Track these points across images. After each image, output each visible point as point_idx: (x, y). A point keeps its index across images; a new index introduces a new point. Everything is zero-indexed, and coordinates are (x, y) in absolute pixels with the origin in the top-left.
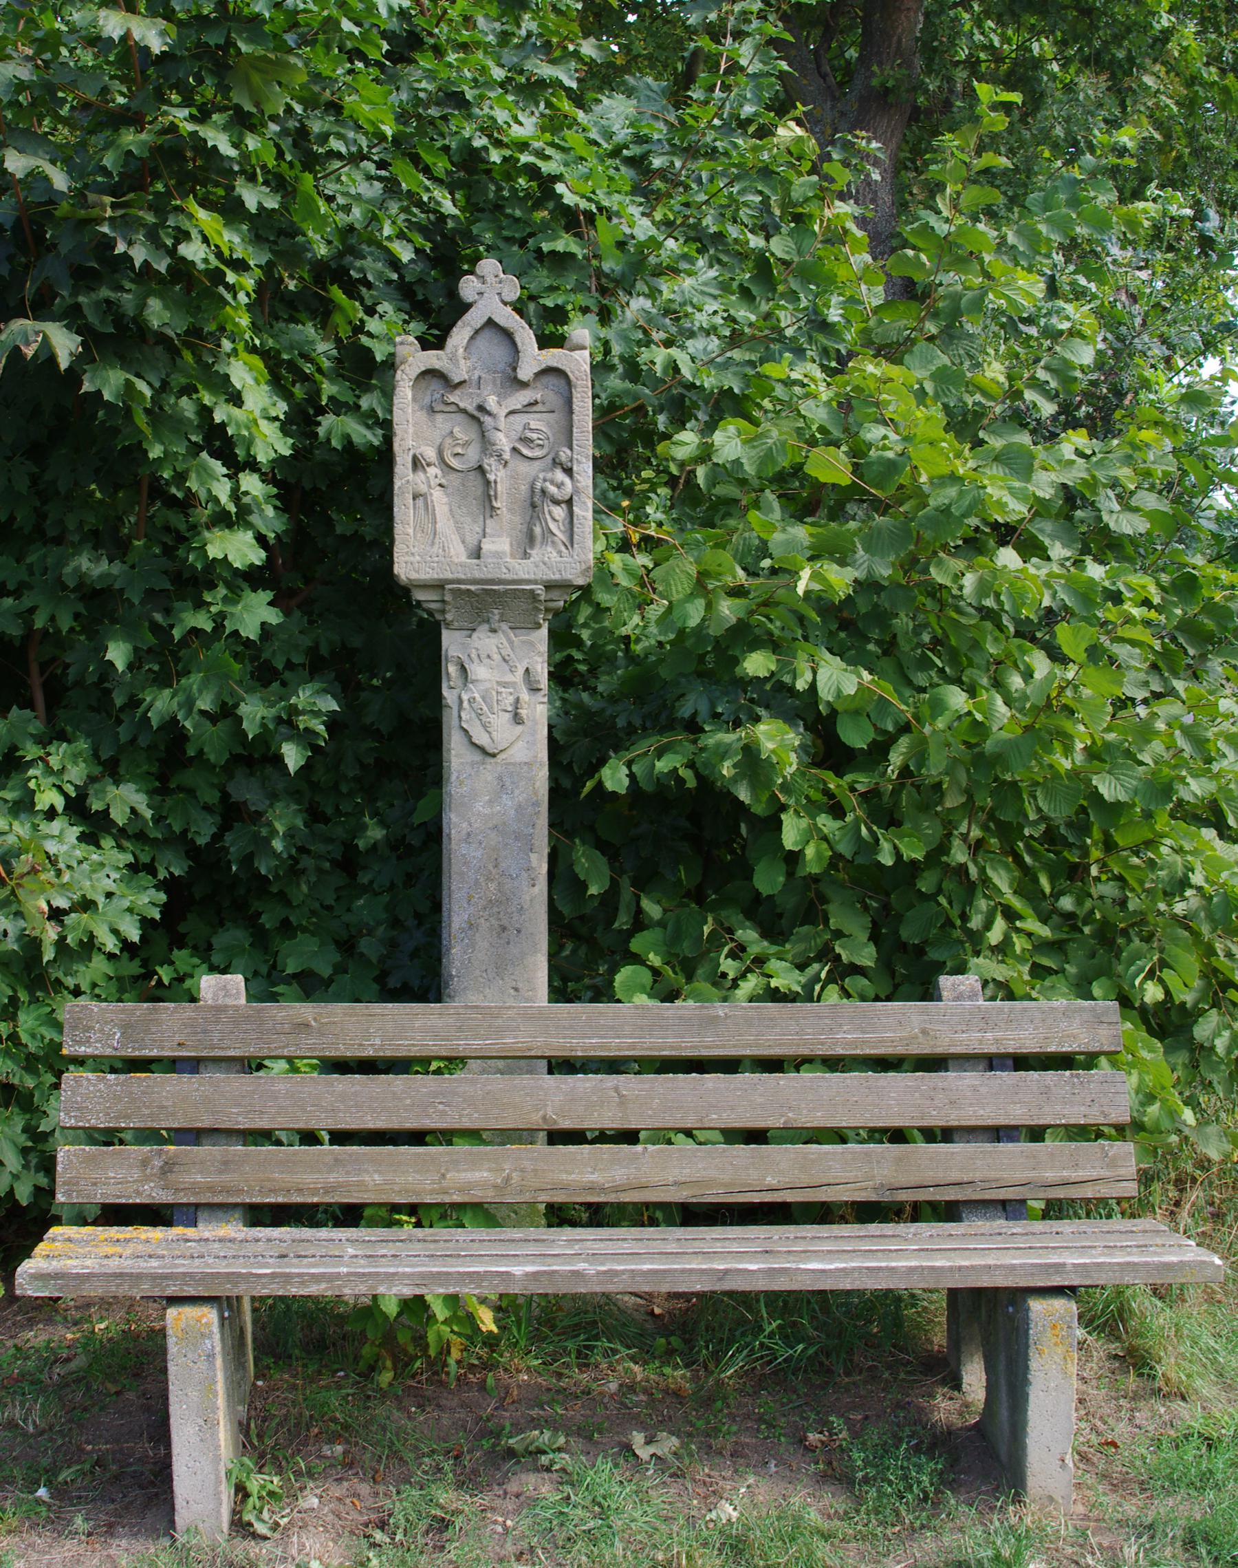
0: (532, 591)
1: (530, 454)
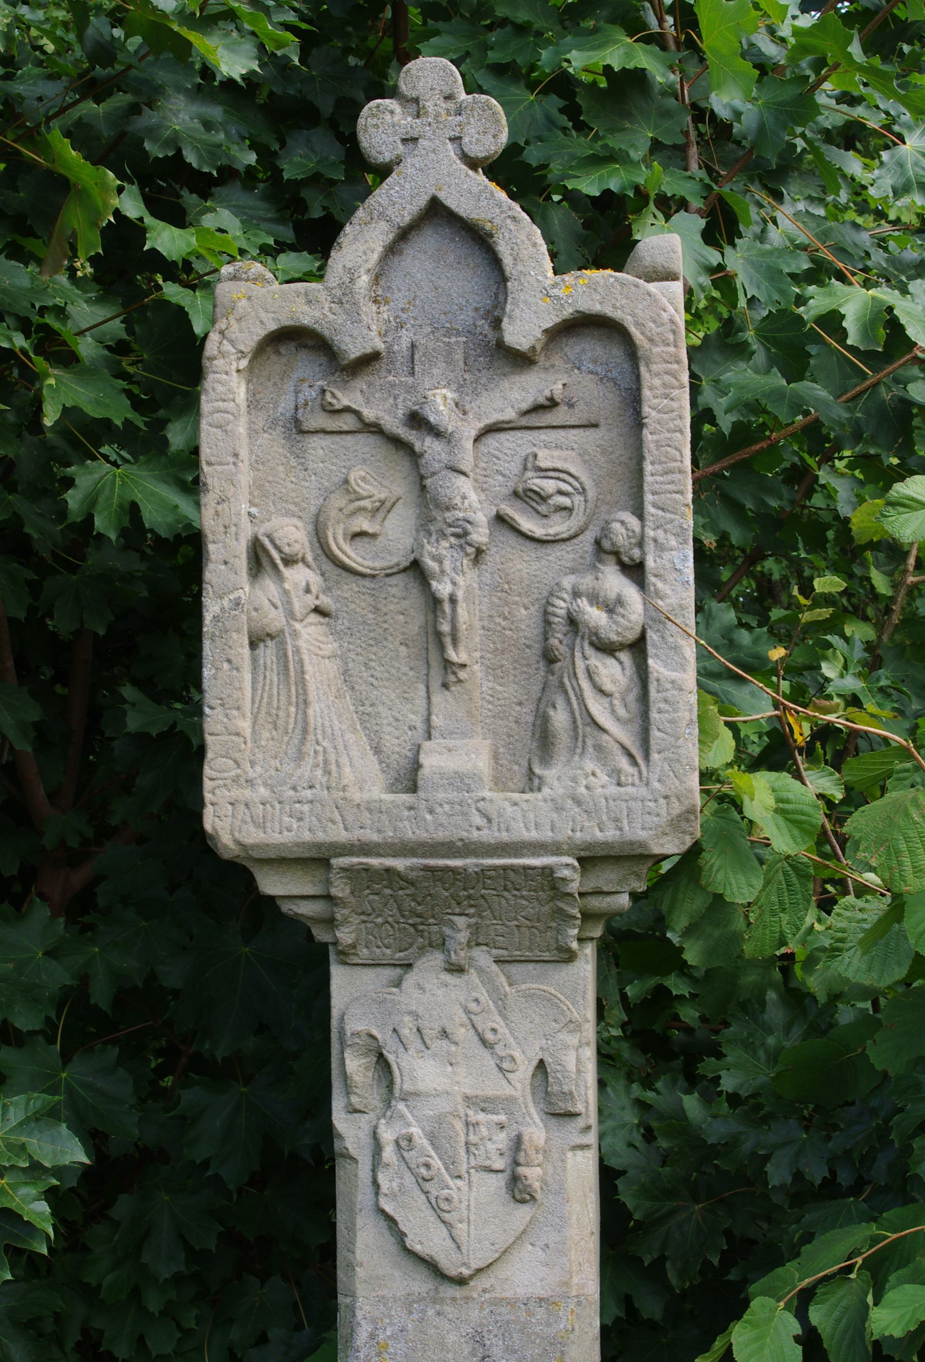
0: (547, 872)
1: (539, 532)
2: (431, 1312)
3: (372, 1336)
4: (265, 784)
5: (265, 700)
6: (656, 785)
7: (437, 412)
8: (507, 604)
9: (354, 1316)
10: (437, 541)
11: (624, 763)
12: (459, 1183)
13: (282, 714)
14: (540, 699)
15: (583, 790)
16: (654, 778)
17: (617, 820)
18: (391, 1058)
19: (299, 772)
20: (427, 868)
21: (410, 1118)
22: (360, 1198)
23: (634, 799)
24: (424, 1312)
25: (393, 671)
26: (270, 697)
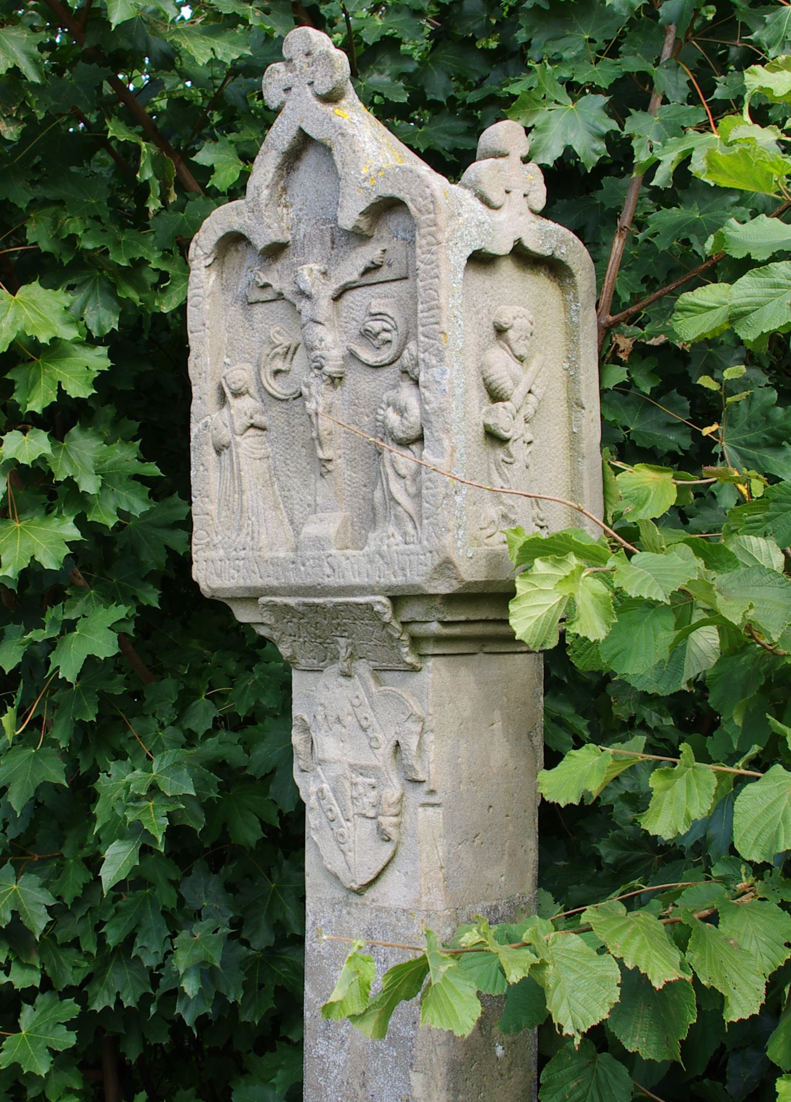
0: (369, 606)
2: (344, 912)
3: (314, 923)
6: (425, 543)
7: (305, 281)
8: (357, 414)
12: (349, 824)
15: (385, 548)
17: (403, 569)
20: (305, 604)
24: (341, 911)
25: (298, 466)
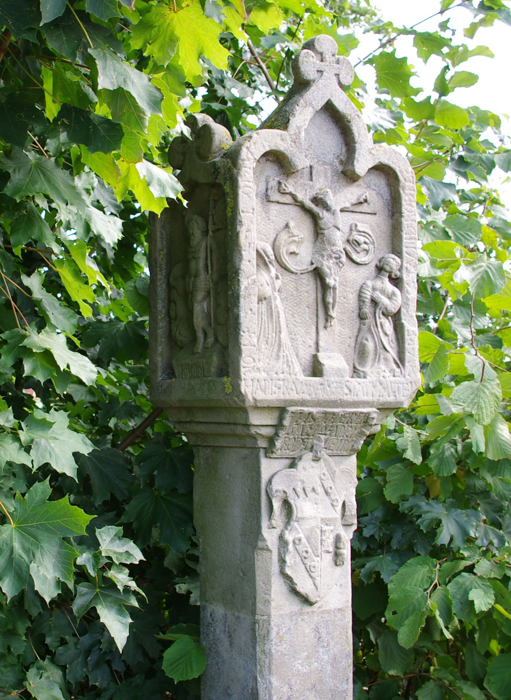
1: (358, 260)
2: (299, 620)
3: (278, 633)
4: (264, 371)
5: (263, 330)
6: (407, 377)
7: (331, 200)
8: (345, 291)
9: (270, 624)
10: (327, 259)
11: (394, 366)
12: (318, 559)
13: (270, 337)
14: (357, 336)
15: (382, 378)
16: (407, 374)
17: (394, 392)
18: (292, 502)
19: (277, 366)
20: (326, 413)
21: (300, 530)
22: (273, 569)
23: (400, 383)
24: (297, 619)
25: (303, 319)
26: (265, 328)
